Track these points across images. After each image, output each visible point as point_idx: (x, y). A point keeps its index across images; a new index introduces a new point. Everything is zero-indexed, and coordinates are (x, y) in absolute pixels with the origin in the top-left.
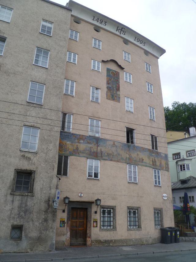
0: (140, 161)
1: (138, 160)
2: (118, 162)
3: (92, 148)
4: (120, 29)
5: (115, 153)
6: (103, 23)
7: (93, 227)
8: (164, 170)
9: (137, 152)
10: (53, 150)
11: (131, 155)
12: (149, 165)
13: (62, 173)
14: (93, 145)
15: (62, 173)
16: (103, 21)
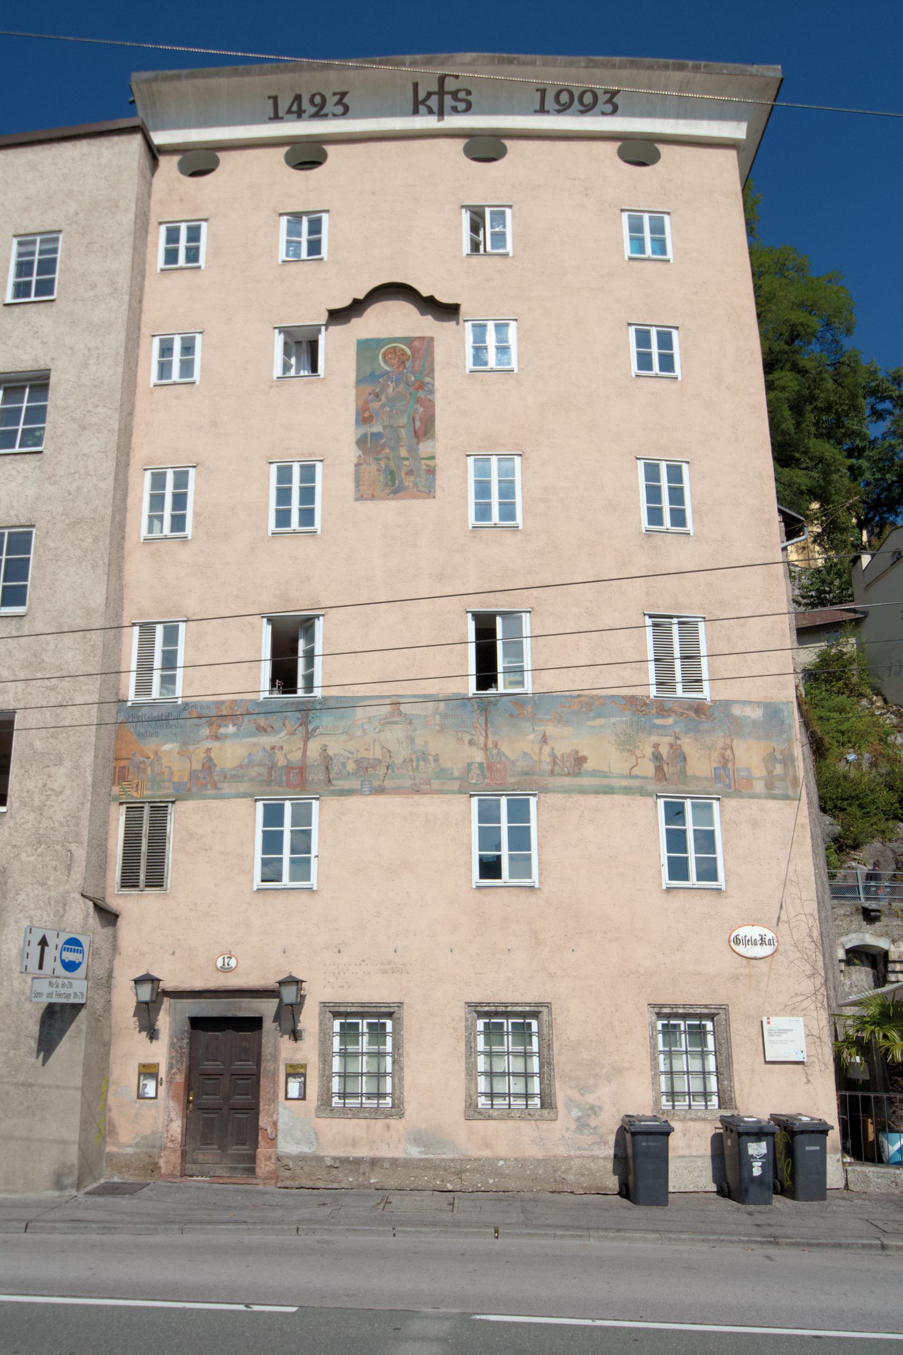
0: (557, 770)
1: (547, 767)
2: (418, 792)
3: (282, 748)
4: (429, 95)
5: (402, 754)
6: (329, 108)
7: (287, 1099)
8: (758, 796)
9: (540, 729)
10: (68, 792)
11: (496, 746)
12: (624, 783)
13: (142, 877)
14: (283, 734)
15: (142, 877)
16: (328, 95)
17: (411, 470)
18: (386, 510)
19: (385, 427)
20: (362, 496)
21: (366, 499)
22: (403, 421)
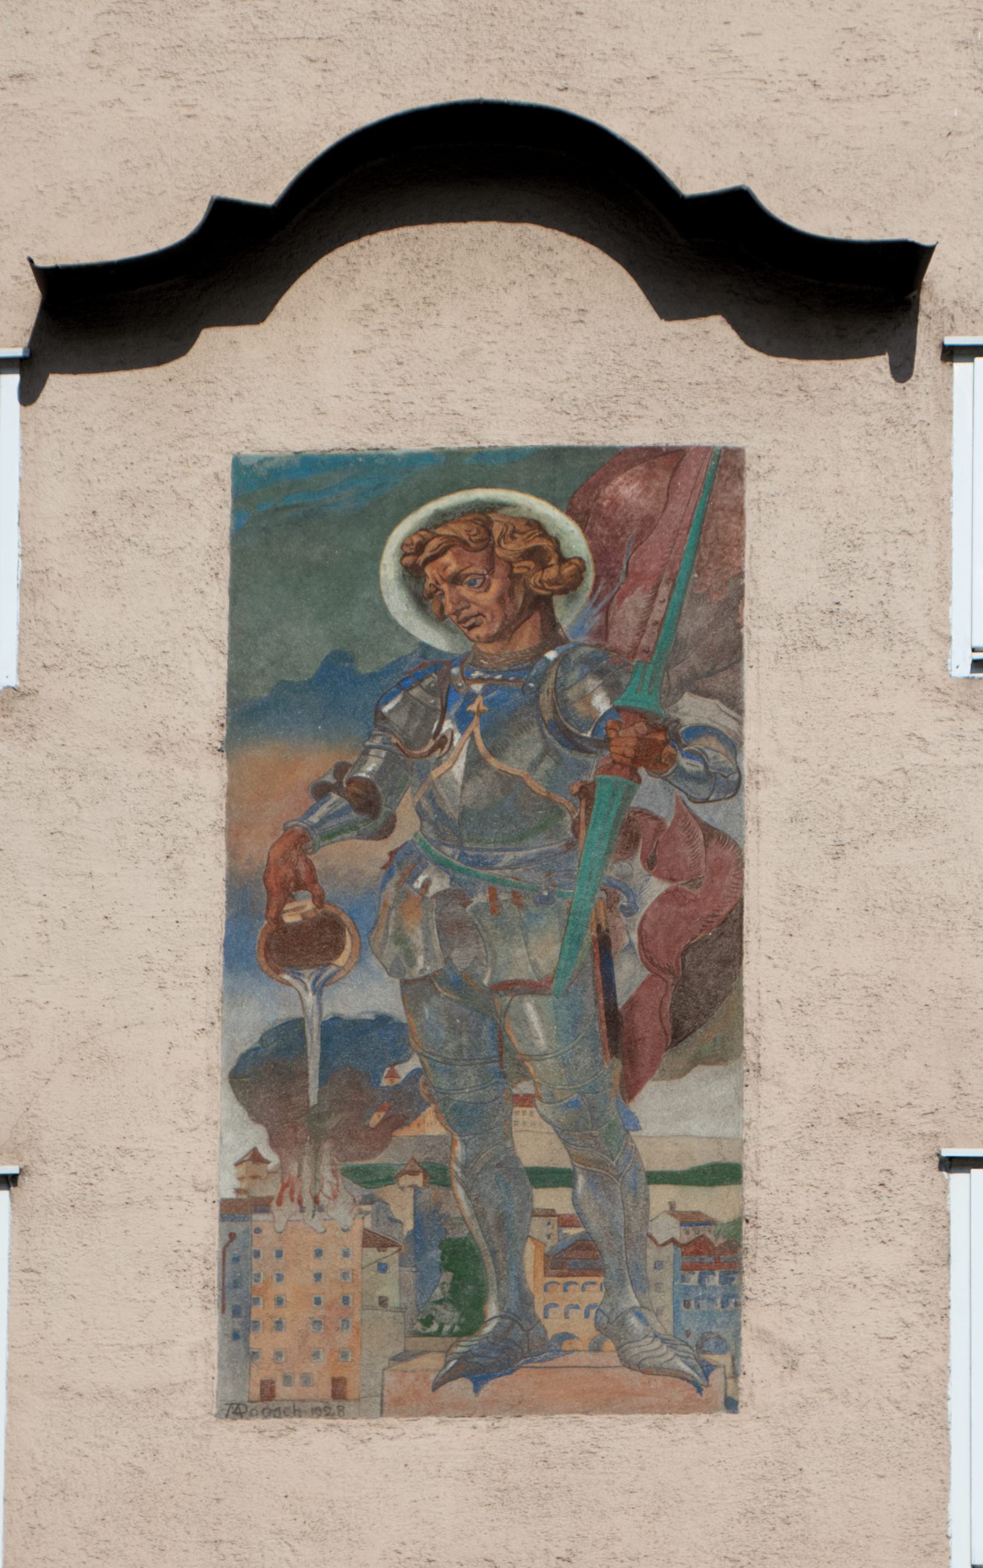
17: (585, 1245)
18: (426, 1469)
19: (415, 991)
20: (268, 1391)
21: (296, 1411)
22: (538, 951)
